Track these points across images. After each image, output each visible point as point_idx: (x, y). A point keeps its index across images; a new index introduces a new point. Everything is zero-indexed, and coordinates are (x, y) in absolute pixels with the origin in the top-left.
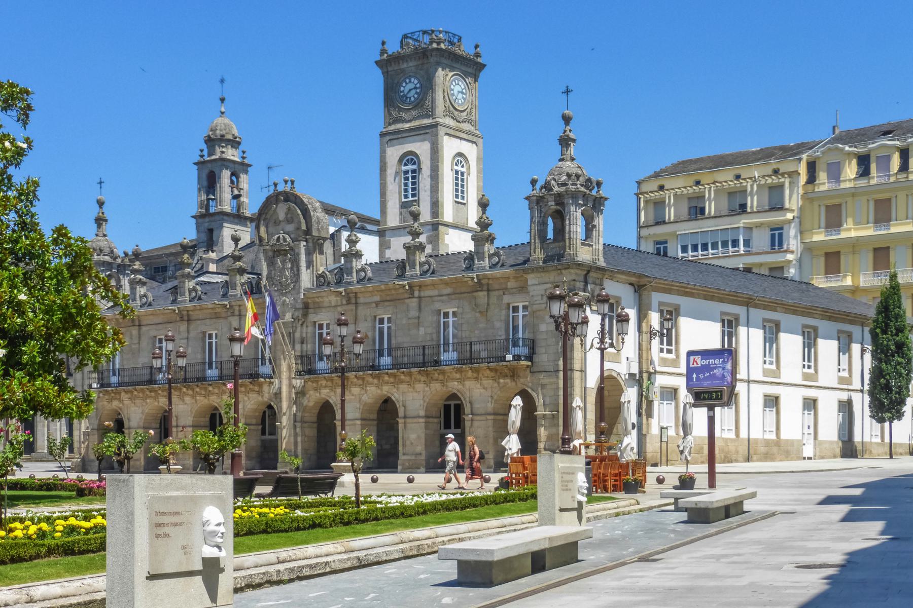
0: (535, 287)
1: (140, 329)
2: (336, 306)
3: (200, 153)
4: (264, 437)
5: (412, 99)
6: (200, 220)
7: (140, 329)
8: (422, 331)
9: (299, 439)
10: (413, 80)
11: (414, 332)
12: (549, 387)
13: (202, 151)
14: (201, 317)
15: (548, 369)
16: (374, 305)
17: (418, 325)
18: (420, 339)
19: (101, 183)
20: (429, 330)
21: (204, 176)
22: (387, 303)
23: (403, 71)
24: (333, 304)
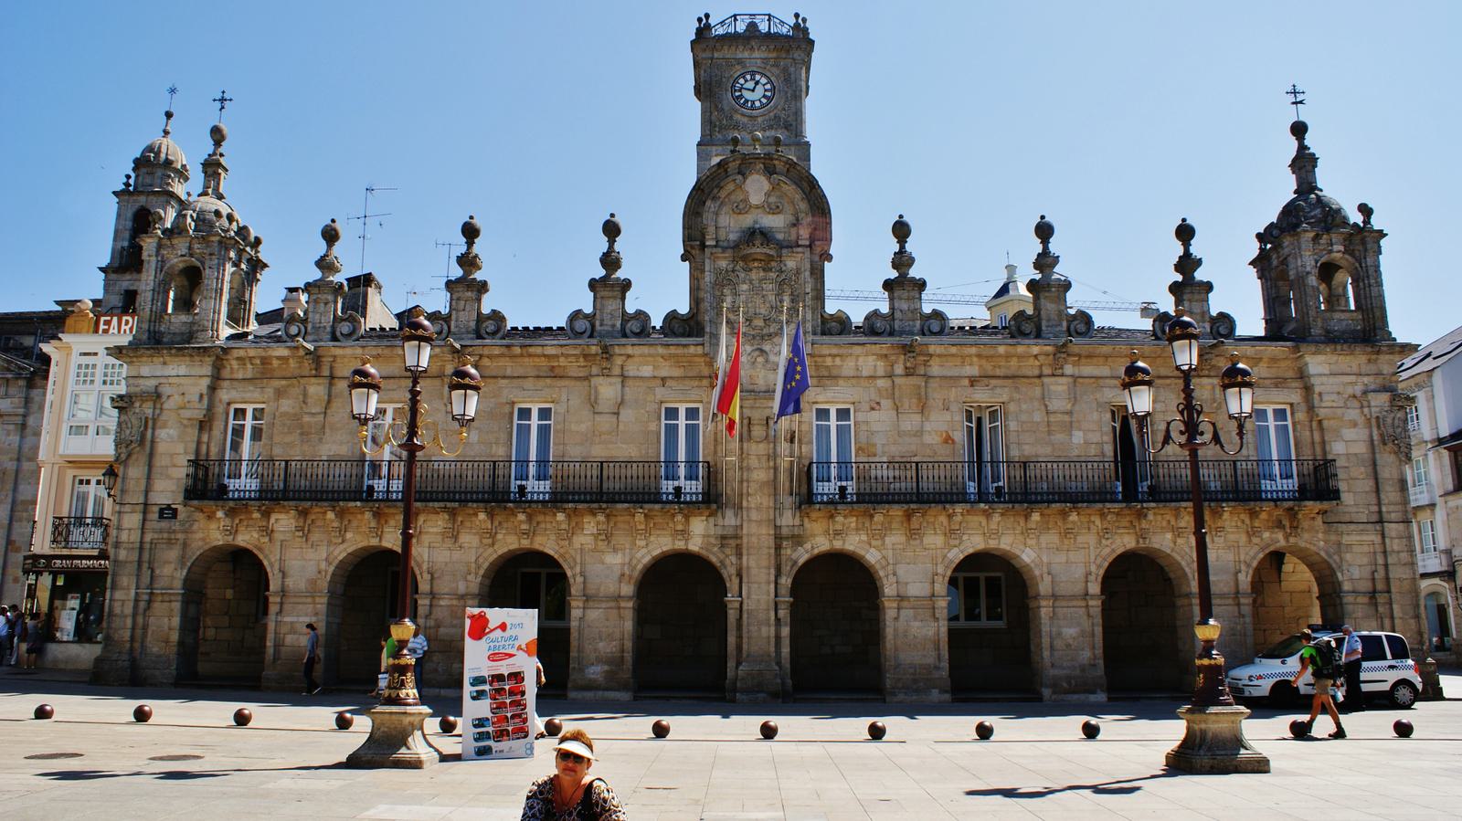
0: (1324, 379)
1: (331, 384)
2: (873, 377)
3: (125, 180)
4: (955, 624)
5: (757, 104)
6: (113, 276)
7: (331, 384)
8: (1078, 437)
9: (786, 631)
10: (758, 77)
11: (1059, 437)
12: (1356, 549)
13: (128, 177)
14: (509, 372)
15: (1355, 518)
16: (966, 382)
17: (1069, 428)
18: (1076, 452)
19: (223, 100)
20: (1095, 438)
21: (130, 214)
22: (994, 382)
23: (740, 62)
24: (865, 373)
